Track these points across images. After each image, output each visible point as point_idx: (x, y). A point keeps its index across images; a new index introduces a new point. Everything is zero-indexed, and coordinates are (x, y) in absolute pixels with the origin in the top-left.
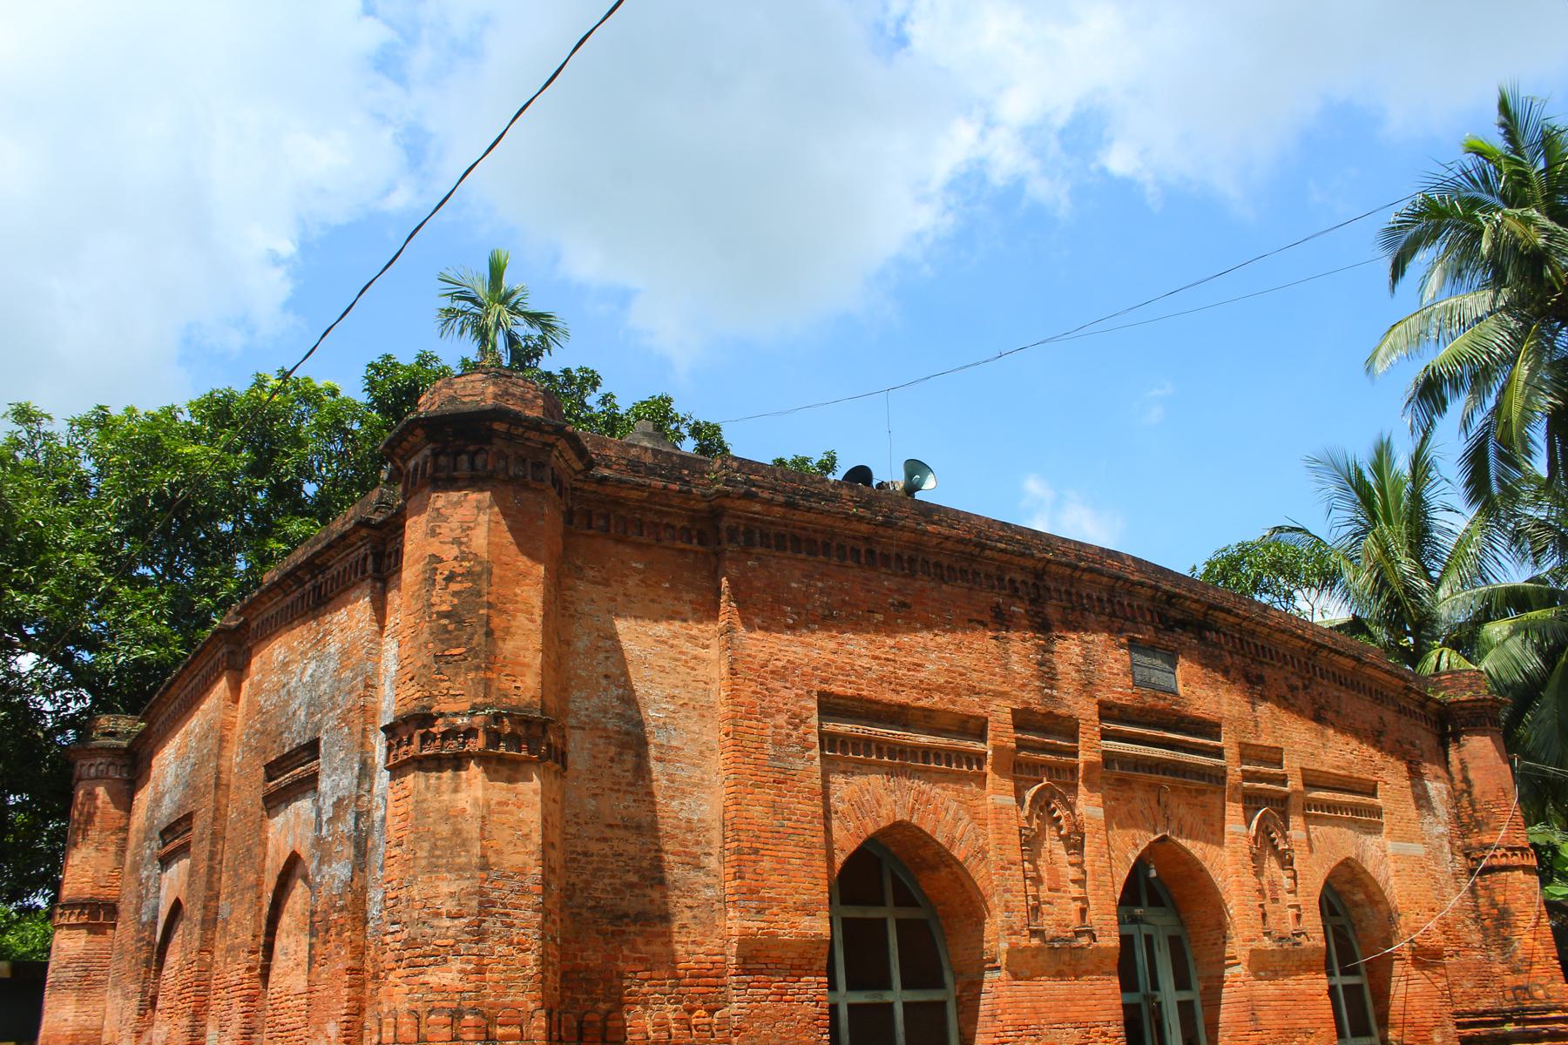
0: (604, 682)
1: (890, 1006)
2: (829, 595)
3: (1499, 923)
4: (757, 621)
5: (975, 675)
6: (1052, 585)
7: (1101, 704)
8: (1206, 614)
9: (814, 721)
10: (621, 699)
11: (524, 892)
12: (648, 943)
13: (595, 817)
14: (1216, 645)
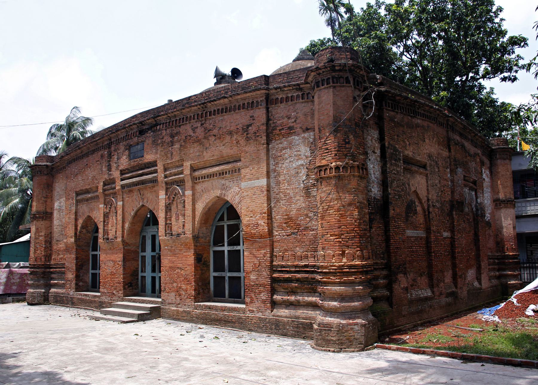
7: (121, 171)
8: (156, 121)
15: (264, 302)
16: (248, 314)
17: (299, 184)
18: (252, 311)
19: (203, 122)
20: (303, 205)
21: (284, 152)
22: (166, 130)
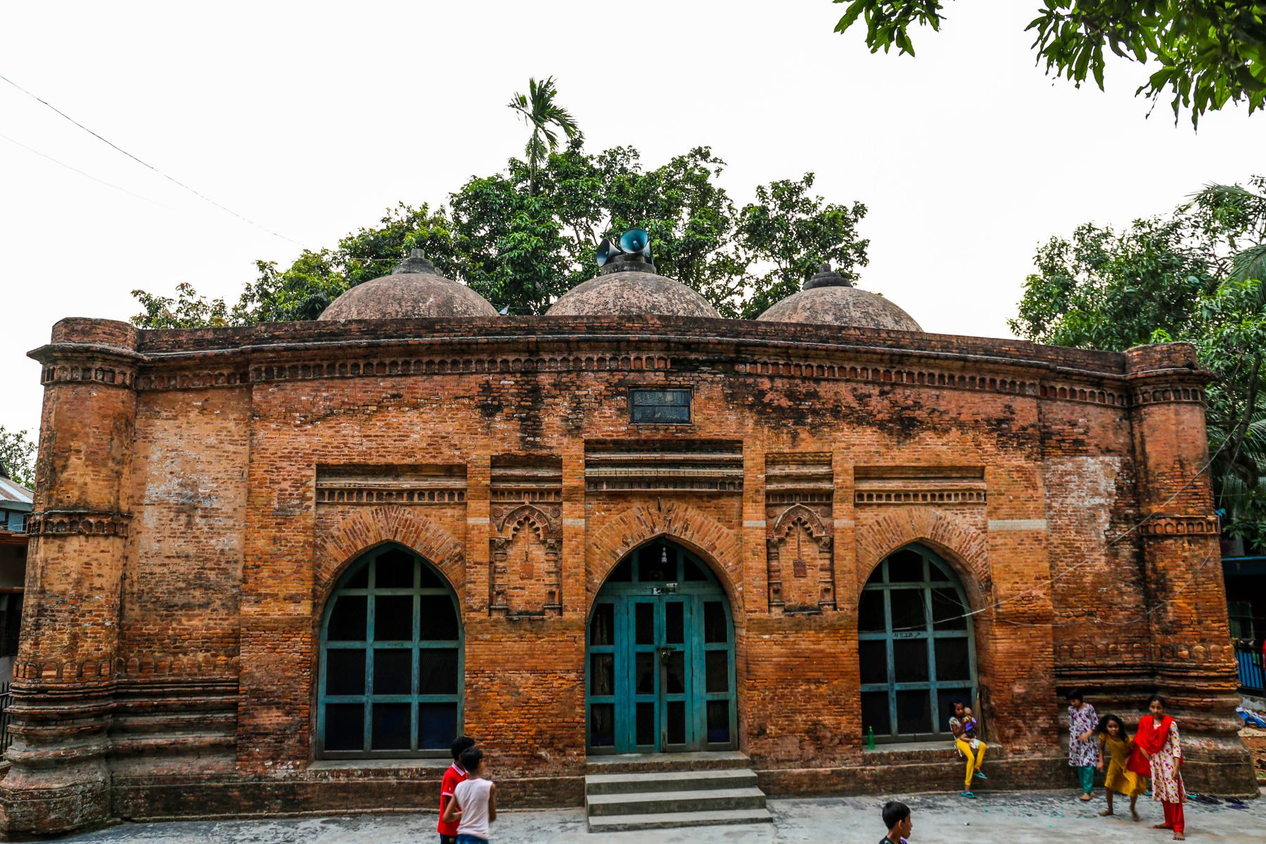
0: (169, 476)
1: (409, 651)
2: (331, 400)
3: (1152, 587)
4: (273, 426)
5: (456, 437)
6: (547, 358)
7: (587, 442)
9: (312, 483)
10: (181, 485)
11: (64, 602)
12: (190, 618)
13: (157, 554)
14: (749, 375)
15: (1044, 732)
16: (1011, 758)
17: (1098, 535)
18: (1021, 752)
19: (887, 388)
20: (1107, 569)
21: (1067, 478)
22: (771, 378)
